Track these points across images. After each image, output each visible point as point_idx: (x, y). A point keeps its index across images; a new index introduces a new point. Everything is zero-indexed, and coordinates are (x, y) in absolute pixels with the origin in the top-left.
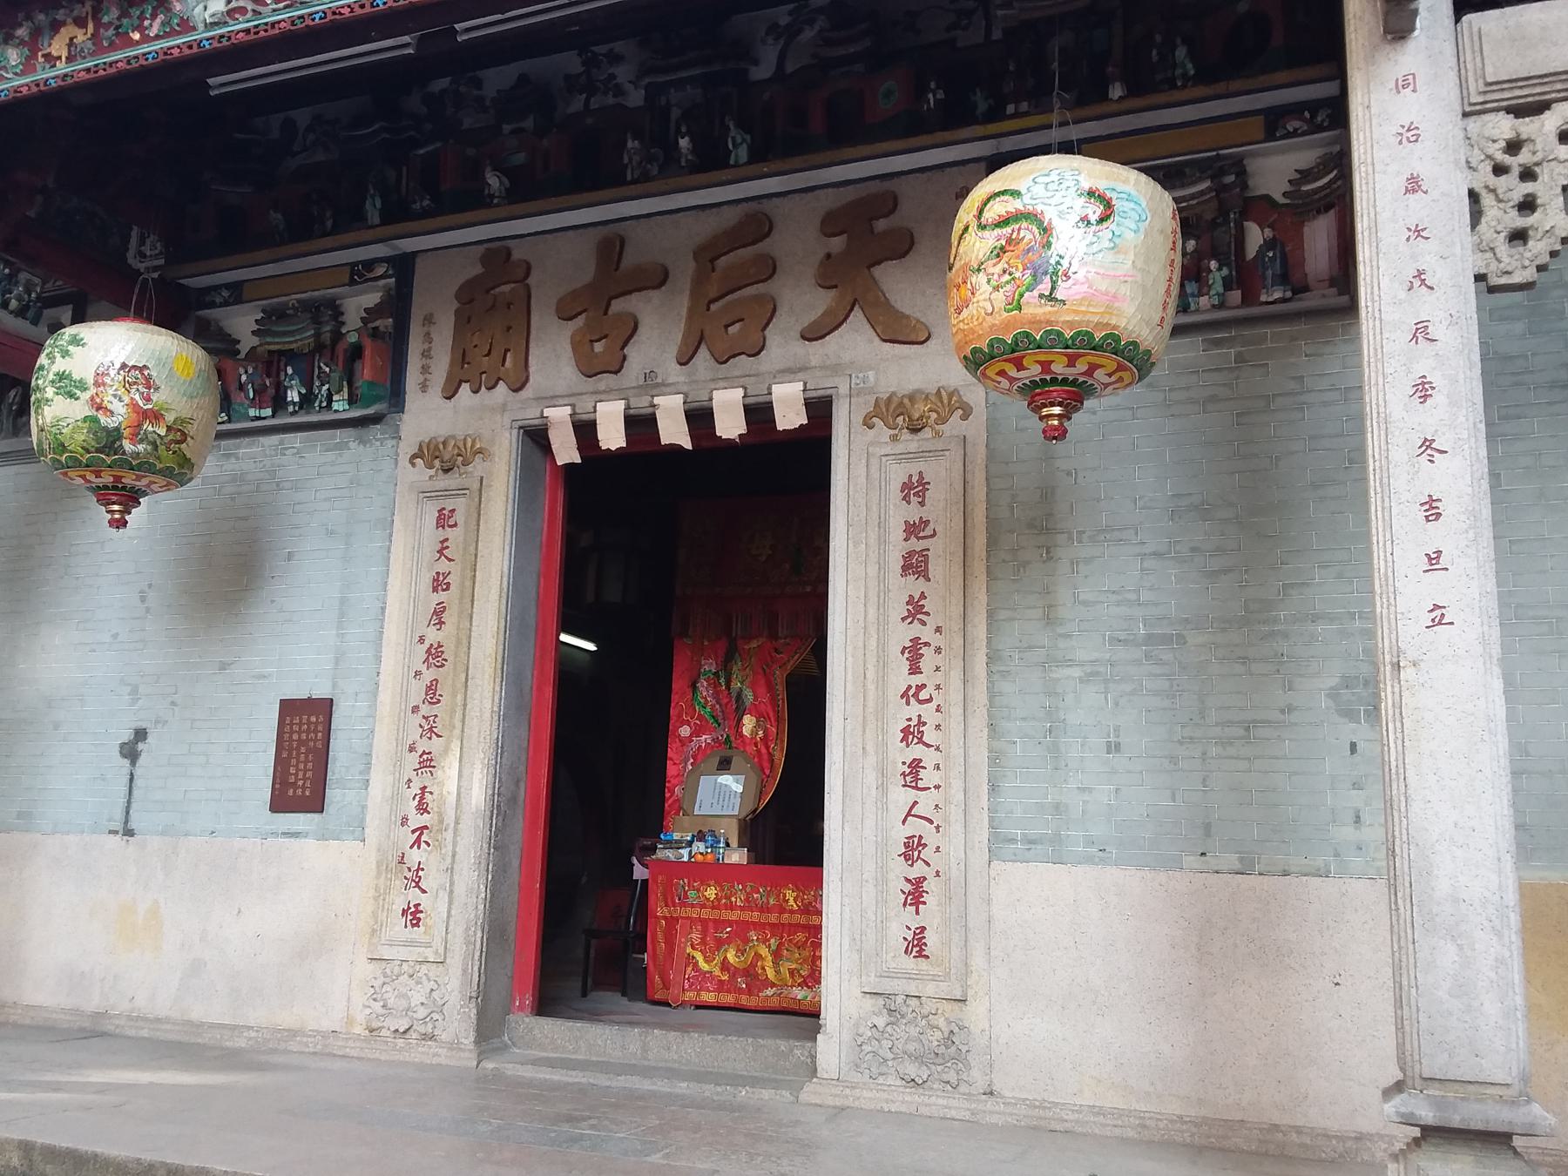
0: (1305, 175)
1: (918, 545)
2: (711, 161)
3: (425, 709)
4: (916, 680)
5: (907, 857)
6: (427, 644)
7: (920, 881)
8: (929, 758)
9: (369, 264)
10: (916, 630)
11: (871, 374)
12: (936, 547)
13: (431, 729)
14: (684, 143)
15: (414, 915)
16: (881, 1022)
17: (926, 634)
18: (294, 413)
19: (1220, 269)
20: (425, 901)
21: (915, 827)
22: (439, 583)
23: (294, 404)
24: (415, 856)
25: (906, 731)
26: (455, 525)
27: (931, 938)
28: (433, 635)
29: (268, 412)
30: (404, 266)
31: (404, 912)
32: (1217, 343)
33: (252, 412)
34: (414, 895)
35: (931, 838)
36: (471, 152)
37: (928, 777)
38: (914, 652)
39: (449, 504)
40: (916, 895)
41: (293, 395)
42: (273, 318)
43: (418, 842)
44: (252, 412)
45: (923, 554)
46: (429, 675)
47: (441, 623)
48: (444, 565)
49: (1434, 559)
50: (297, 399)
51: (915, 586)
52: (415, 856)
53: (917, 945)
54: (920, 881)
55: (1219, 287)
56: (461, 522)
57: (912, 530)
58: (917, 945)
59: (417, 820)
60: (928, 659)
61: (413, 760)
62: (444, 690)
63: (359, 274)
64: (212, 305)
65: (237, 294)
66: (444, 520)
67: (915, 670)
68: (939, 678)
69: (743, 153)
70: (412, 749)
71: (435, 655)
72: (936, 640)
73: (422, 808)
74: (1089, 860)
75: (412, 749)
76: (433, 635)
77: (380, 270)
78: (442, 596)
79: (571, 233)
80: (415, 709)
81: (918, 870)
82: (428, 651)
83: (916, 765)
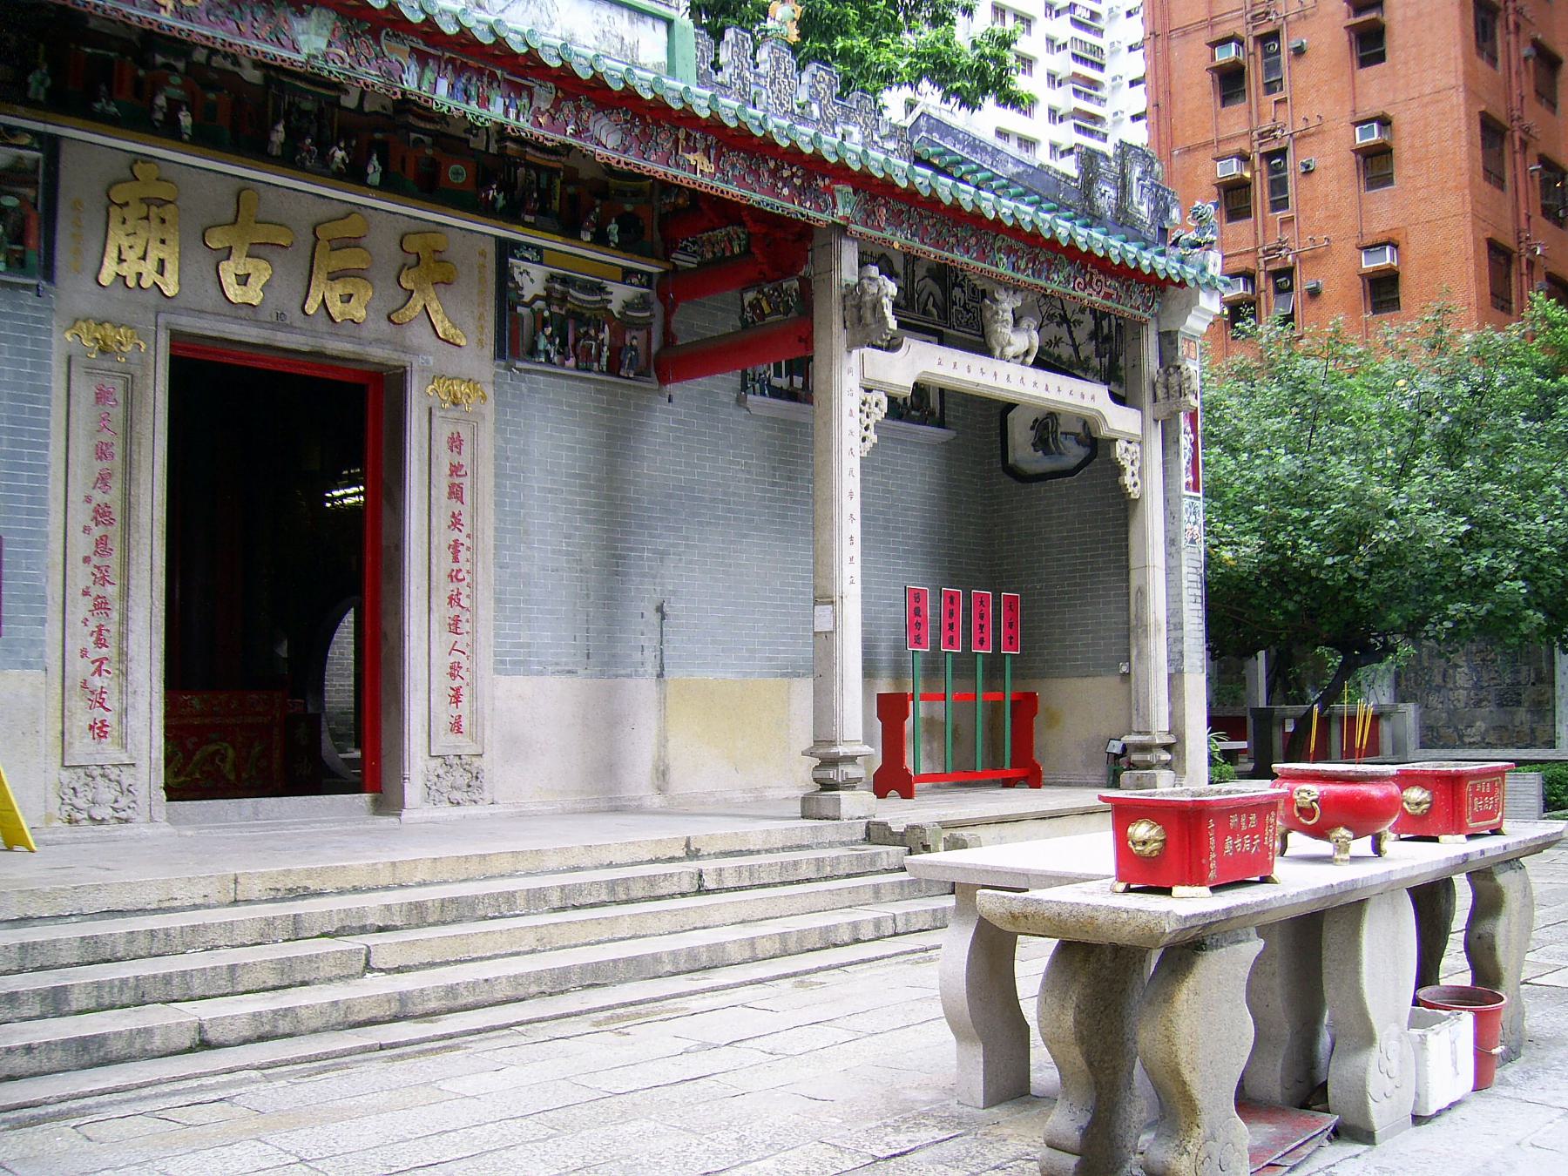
0: (628, 305)
1: (457, 481)
2: (353, 175)
3: (96, 560)
4: (456, 566)
5: (452, 675)
6: (94, 505)
7: (457, 690)
8: (465, 616)
10: (455, 534)
11: (431, 359)
12: (466, 482)
13: (103, 578)
14: (339, 154)
15: (99, 730)
16: (441, 772)
17: (462, 538)
20: (111, 718)
21: (457, 656)
24: (97, 682)
25: (451, 598)
27: (465, 723)
28: (99, 497)
30: (52, 145)
31: (91, 728)
32: (598, 391)
34: (99, 713)
35: (465, 664)
37: (464, 627)
38: (455, 547)
39: (108, 383)
40: (456, 698)
43: (99, 671)
45: (460, 486)
46: (98, 531)
48: (106, 437)
51: (456, 506)
52: (97, 682)
53: (456, 727)
54: (457, 690)
57: (455, 470)
58: (456, 727)
59: (96, 653)
60: (464, 554)
61: (88, 603)
62: (115, 544)
66: (101, 396)
67: (456, 560)
68: (468, 566)
70: (86, 593)
72: (467, 542)
73: (101, 643)
74: (541, 673)
75: (86, 593)
76: (99, 497)
77: (26, 140)
78: (106, 464)
79: (212, 175)
80: (86, 560)
81: (457, 683)
82: (96, 511)
83: (457, 620)
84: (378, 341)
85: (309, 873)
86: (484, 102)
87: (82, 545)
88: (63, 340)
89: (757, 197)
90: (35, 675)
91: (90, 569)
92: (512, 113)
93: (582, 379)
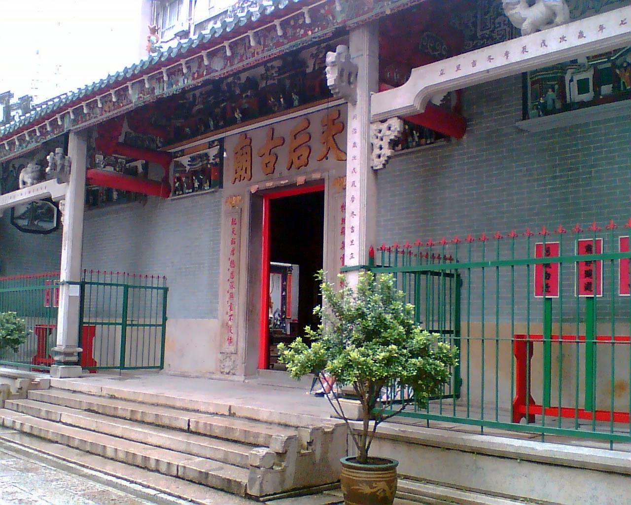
2: (290, 106)
3: (231, 280)
9: (213, 142)
15: (230, 340)
18: (197, 191)
19: (417, 133)
20: (232, 336)
22: (233, 242)
23: (196, 188)
24: (230, 323)
26: (236, 224)
29: (191, 190)
30: (221, 141)
33: (187, 191)
36: (233, 105)
41: (196, 185)
42: (193, 159)
43: (230, 319)
44: (187, 191)
46: (231, 270)
47: (234, 254)
49: (352, 242)
50: (197, 186)
55: (417, 139)
56: (237, 222)
59: (229, 314)
61: (228, 295)
63: (211, 145)
64: (177, 157)
65: (183, 153)
69: (296, 103)
71: (232, 263)
73: (231, 309)
76: (232, 258)
77: (216, 144)
84: (314, 171)
85: (116, 391)
86: (177, 82)
87: (229, 276)
88: (224, 207)
89: (287, 46)
90: (216, 320)
91: (229, 283)
92: (186, 82)
93: (407, 154)
